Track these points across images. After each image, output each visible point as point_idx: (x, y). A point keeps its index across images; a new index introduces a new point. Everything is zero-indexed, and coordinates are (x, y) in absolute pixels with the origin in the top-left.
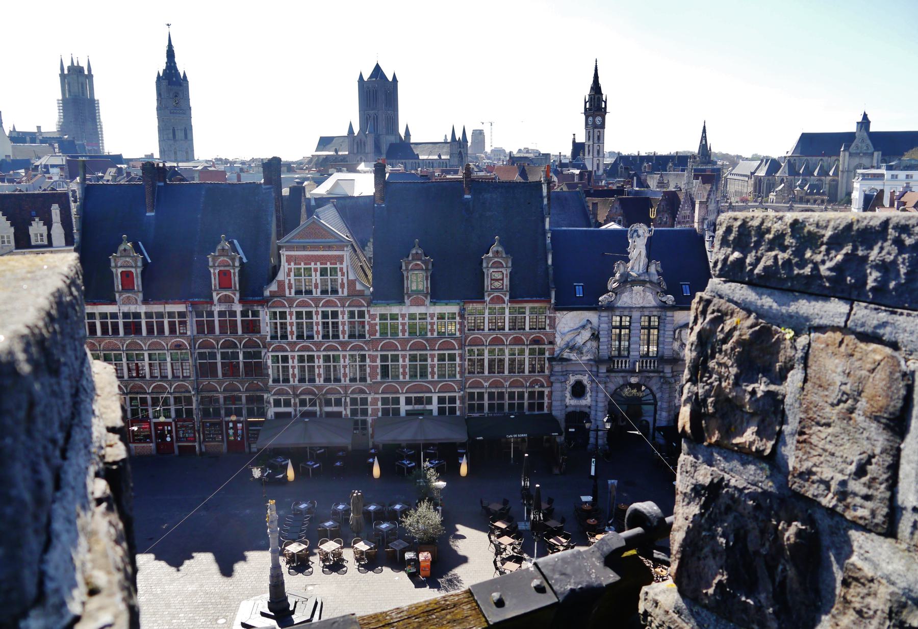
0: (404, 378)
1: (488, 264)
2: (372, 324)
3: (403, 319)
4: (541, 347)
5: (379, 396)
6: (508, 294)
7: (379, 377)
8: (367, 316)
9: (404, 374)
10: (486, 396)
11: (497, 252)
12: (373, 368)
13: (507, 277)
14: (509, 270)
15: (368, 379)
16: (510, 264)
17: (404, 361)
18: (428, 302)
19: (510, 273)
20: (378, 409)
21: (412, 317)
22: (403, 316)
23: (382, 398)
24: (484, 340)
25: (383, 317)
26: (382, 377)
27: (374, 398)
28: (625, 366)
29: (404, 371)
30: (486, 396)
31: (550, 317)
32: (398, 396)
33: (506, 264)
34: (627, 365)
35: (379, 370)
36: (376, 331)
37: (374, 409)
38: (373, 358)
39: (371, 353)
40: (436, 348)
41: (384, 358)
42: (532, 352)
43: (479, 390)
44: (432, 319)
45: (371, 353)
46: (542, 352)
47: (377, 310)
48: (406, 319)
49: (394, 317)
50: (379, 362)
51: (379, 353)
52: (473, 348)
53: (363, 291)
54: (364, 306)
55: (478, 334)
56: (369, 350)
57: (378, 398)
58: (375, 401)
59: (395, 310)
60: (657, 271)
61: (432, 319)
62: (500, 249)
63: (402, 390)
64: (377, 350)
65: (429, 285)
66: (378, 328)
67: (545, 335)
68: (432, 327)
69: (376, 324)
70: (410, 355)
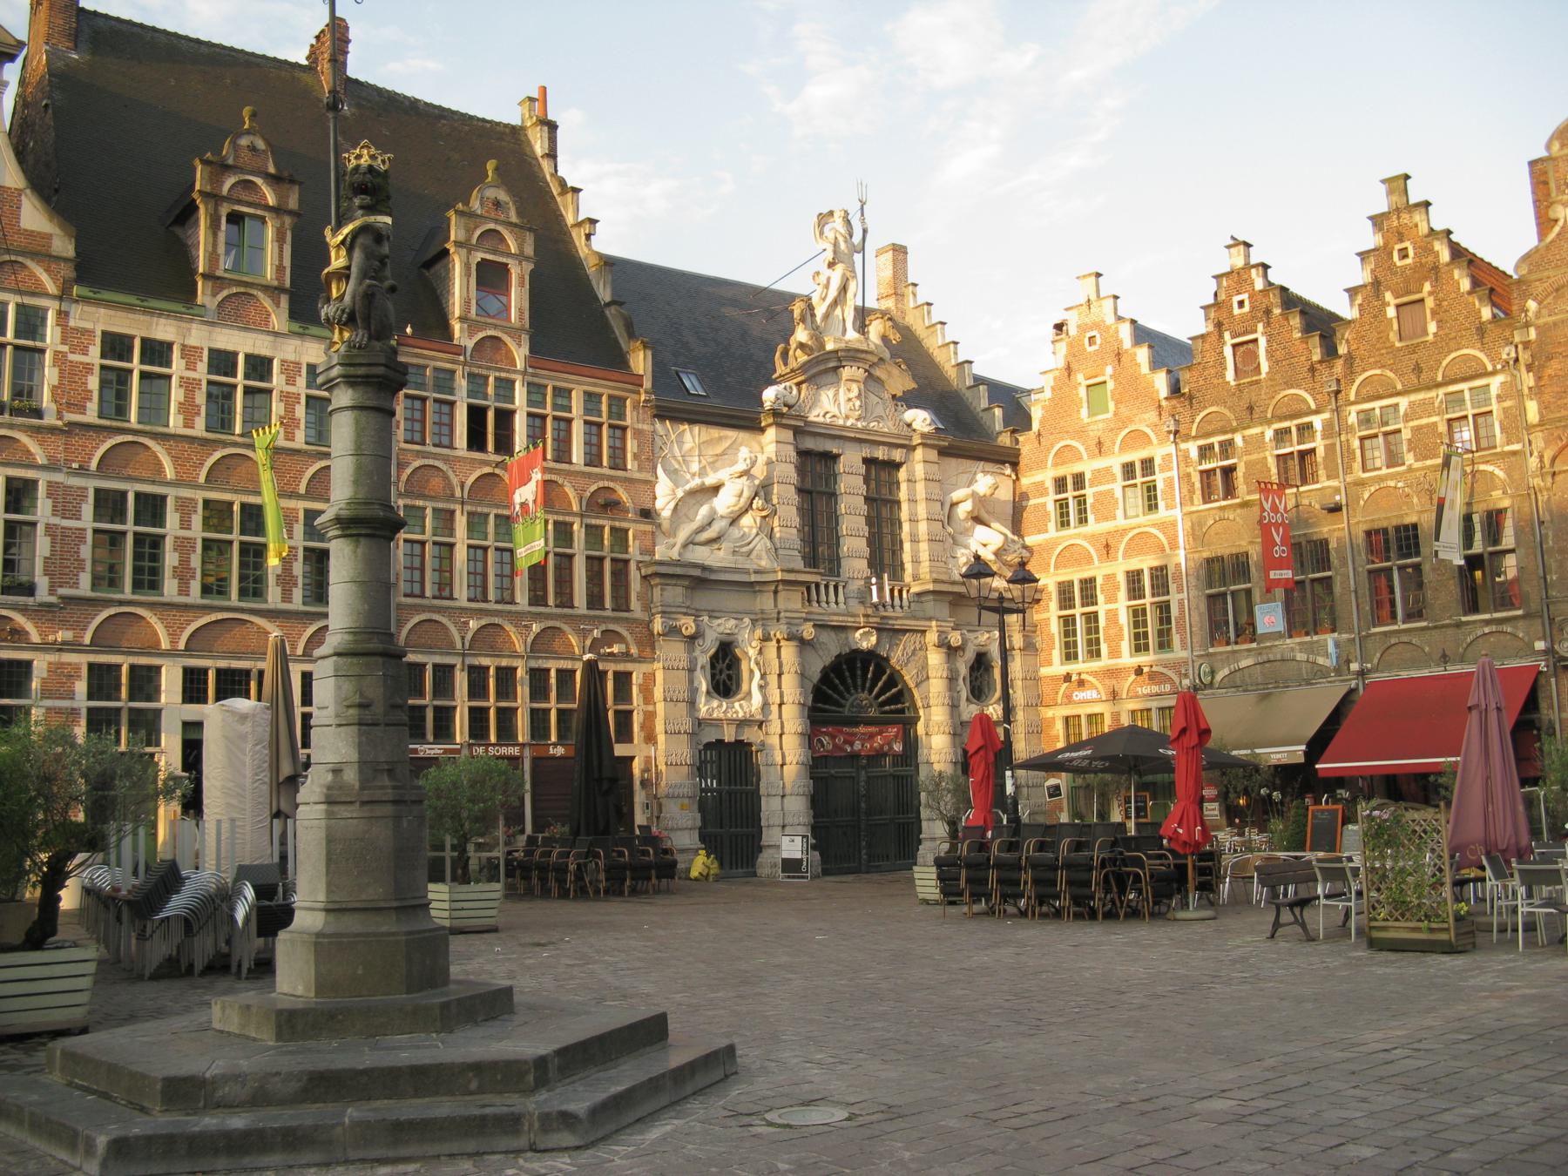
0: (184, 590)
1: (470, 232)
2: (73, 364)
3: (191, 366)
4: (617, 524)
5: (83, 660)
6: (525, 338)
7: (85, 579)
8: (52, 333)
9: (183, 573)
10: (461, 681)
11: (497, 204)
12: (64, 540)
13: (521, 284)
14: (528, 267)
15: (42, 582)
16: (529, 250)
17: (185, 524)
18: (279, 319)
19: (532, 273)
20: (74, 712)
21: (222, 361)
22: (189, 353)
23: (91, 666)
24: (455, 481)
25: (116, 345)
26: (96, 582)
27: (61, 665)
28: (837, 603)
29: (184, 562)
30: (461, 681)
31: (638, 433)
32: (155, 661)
33: (521, 246)
34: (841, 598)
35: (86, 551)
36: (87, 396)
37: (59, 711)
38: (65, 503)
39: (58, 477)
40: (302, 489)
41: (109, 504)
42: (593, 533)
43: (438, 659)
44: (291, 381)
45: (58, 477)
46: (620, 535)
47: (99, 319)
48: (202, 367)
49: (157, 352)
50: (87, 519)
51: (91, 484)
52: (420, 503)
53: (49, 237)
54: (46, 295)
55: (435, 456)
56: (51, 467)
57: (77, 667)
58: (59, 684)
59: (163, 330)
60: (884, 338)
61: (291, 381)
62: (503, 196)
63: (174, 638)
64: (83, 471)
65: (287, 262)
66: (93, 383)
67: (630, 481)
68: (290, 409)
69: (88, 368)
70: (207, 503)
